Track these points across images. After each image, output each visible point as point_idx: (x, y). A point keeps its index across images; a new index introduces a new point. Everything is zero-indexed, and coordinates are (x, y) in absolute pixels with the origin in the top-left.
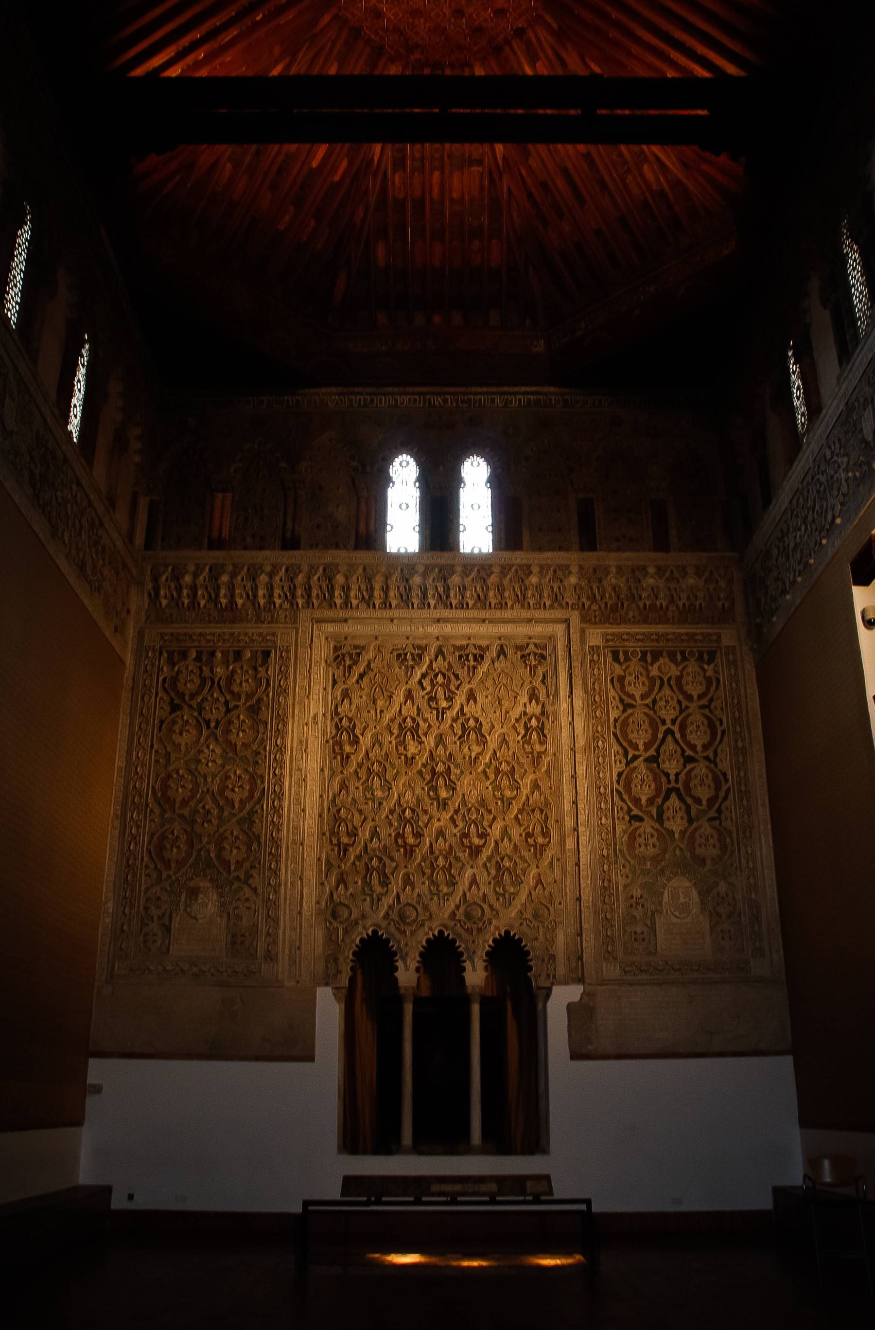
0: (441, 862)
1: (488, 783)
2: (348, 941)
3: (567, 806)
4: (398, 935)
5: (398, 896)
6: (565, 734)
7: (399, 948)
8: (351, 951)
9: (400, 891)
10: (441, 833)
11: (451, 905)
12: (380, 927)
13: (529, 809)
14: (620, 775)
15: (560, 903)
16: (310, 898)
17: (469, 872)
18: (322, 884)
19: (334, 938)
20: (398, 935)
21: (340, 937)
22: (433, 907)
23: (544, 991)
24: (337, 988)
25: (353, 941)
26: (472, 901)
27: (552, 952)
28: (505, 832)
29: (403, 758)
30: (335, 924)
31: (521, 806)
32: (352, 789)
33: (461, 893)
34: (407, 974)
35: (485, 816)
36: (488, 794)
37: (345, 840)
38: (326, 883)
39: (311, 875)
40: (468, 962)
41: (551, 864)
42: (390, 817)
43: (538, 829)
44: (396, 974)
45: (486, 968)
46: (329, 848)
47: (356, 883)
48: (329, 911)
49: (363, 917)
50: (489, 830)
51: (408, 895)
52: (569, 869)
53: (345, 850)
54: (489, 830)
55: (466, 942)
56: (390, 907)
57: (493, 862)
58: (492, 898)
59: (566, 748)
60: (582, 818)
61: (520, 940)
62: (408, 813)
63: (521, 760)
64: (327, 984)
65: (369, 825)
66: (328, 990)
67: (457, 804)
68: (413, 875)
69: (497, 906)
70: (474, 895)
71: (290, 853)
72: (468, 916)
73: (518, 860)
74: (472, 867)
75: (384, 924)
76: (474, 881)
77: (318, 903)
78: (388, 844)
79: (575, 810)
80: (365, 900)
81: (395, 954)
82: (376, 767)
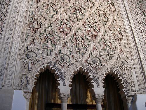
0: (80, 39)
1: (96, 16)
2: (33, 69)
3: (127, 27)
4: (60, 68)
5: (60, 51)
6: (122, 6)
7: (61, 75)
8: (35, 74)
9: (61, 49)
10: (79, 28)
11: (85, 57)
12: (51, 64)
13: (113, 26)
14: (144, 19)
15: (132, 60)
16: (17, 46)
17: (92, 44)
18: (23, 42)
19: (26, 67)
20: (60, 68)
21: (30, 67)
22: (77, 56)
23: (131, 98)
24: (26, 93)
25: (36, 69)
26: (95, 56)
27: (132, 80)
28: (105, 32)
29: (62, 3)
30: (28, 60)
31: (110, 25)
32: (41, 10)
33: (89, 53)
34: (64, 88)
35: (96, 26)
36: (97, 19)
37: (36, 26)
38: (25, 41)
39: (18, 38)
40: (95, 83)
41: (125, 45)
42: (57, 21)
43: (117, 33)
44: (58, 87)
45: (104, 86)
46: (28, 28)
47: (40, 43)
48: (25, 54)
49: (43, 58)
50: (99, 31)
51: (65, 51)
52: (132, 48)
53: (35, 31)
54: (99, 31)
55: (94, 73)
56: (56, 55)
57: (102, 41)
58: (103, 55)
59: (123, 10)
60: (134, 30)
61: (117, 75)
62: (65, 21)
63: (107, 11)
64: (21, 89)
65: (47, 23)
66: (22, 91)
67: (85, 21)
68: (67, 43)
69: (106, 59)
70: (95, 53)
71: (9, 26)
72: (94, 62)
73: (112, 42)
74: (94, 42)
75: (53, 62)
76: (95, 48)
77: (20, 50)
78: (56, 30)
79: (130, 28)
80: (44, 50)
81: (58, 77)
82: (51, 4)
